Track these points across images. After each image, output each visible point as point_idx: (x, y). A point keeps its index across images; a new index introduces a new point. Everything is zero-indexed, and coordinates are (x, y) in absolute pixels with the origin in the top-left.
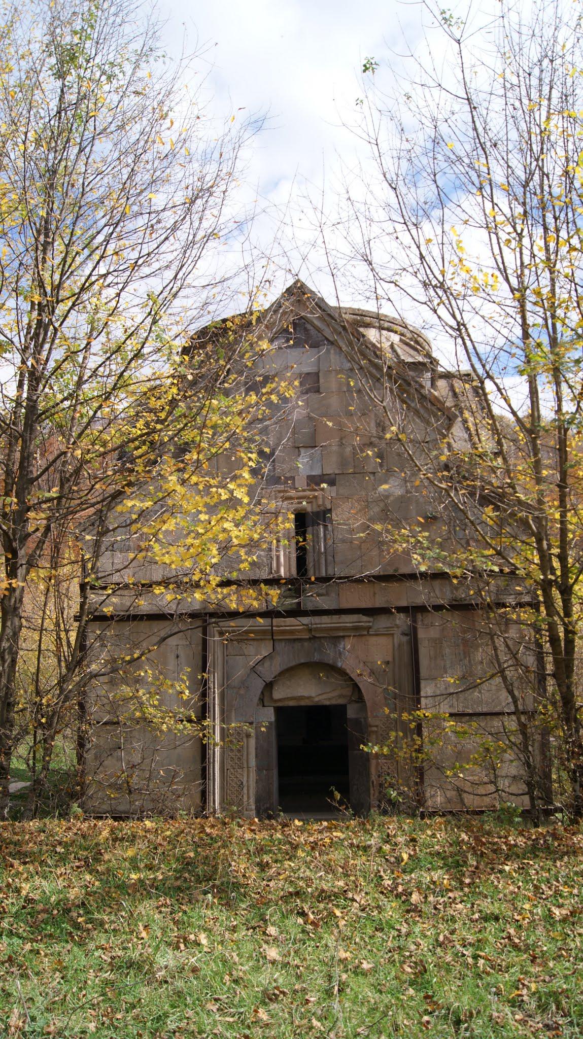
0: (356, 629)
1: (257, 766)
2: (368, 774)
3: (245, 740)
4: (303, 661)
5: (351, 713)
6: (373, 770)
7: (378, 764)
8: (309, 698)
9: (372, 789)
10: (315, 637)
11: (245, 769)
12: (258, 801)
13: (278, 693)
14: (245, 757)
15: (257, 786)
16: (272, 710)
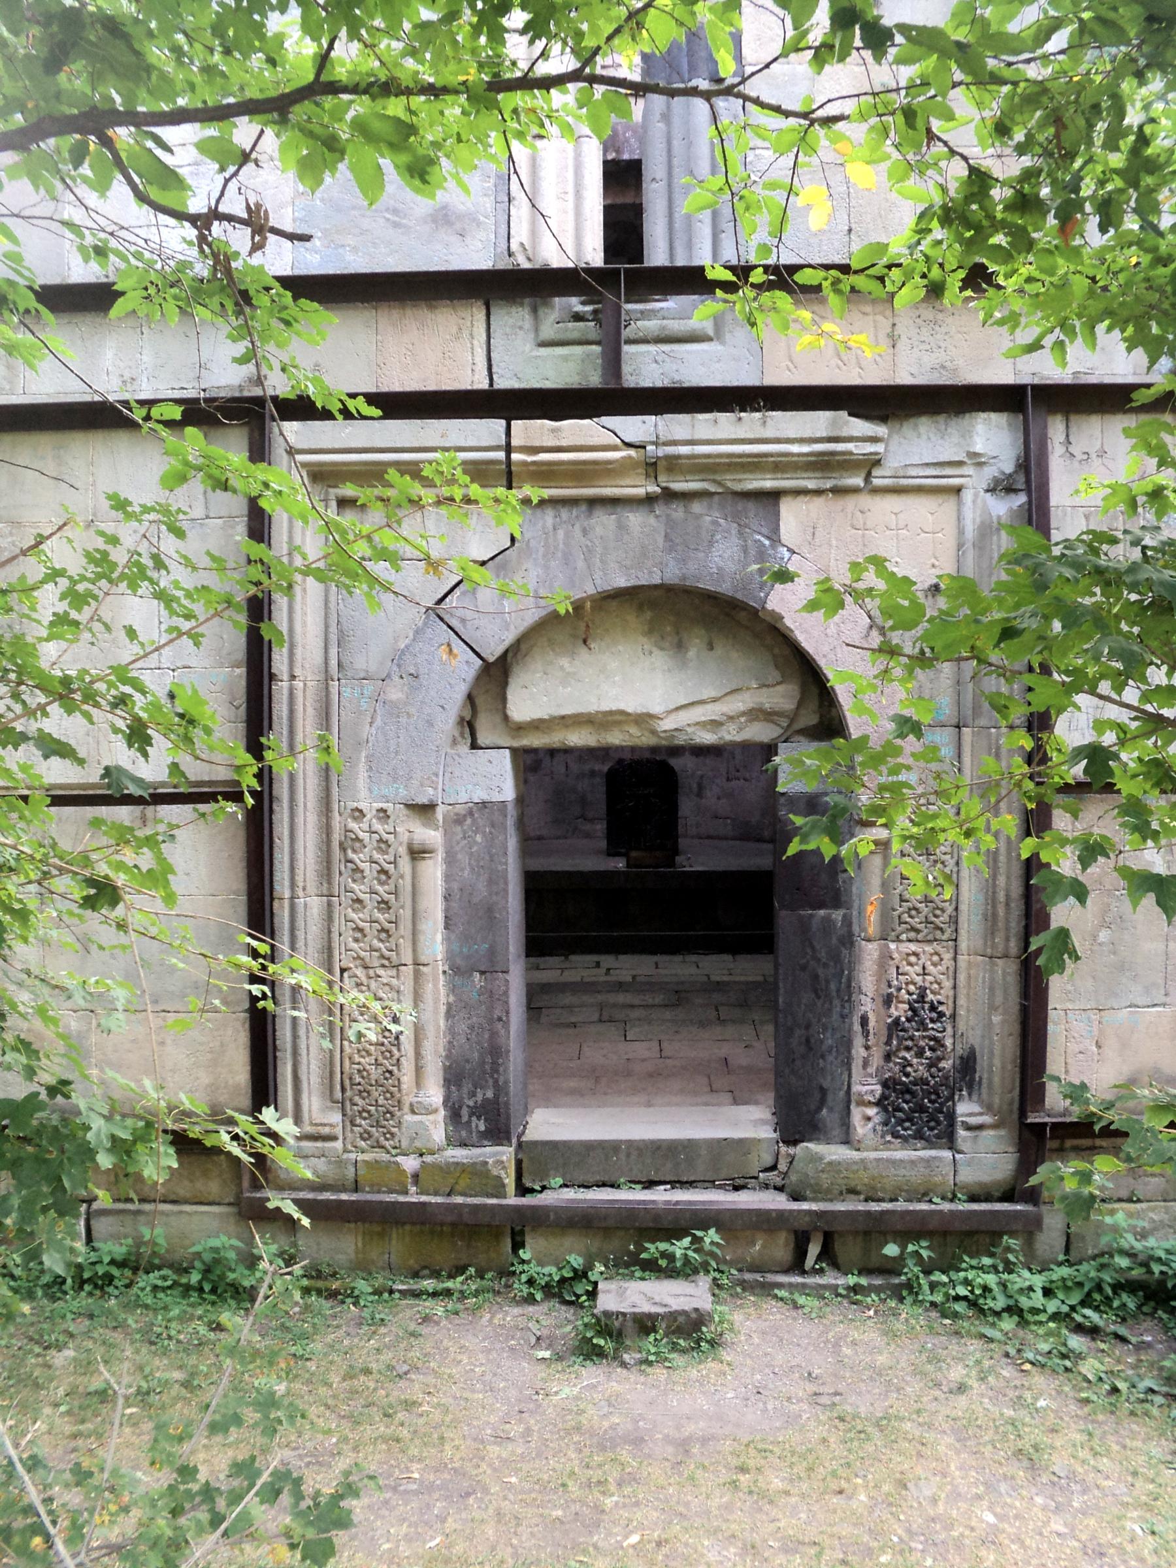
0: (824, 464)
1: (450, 957)
2: (848, 991)
3: (405, 865)
4: (622, 582)
5: (798, 769)
6: (867, 981)
7: (886, 956)
8: (644, 719)
9: (858, 1041)
10: (669, 495)
11: (408, 971)
12: (453, 1078)
13: (533, 698)
14: (405, 928)
15: (451, 1030)
16: (504, 760)
